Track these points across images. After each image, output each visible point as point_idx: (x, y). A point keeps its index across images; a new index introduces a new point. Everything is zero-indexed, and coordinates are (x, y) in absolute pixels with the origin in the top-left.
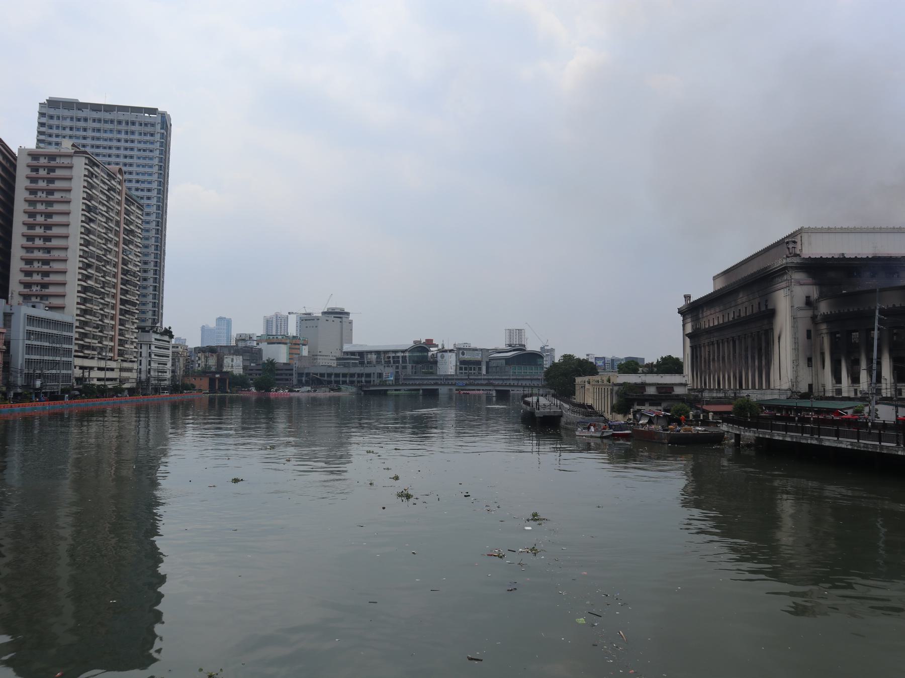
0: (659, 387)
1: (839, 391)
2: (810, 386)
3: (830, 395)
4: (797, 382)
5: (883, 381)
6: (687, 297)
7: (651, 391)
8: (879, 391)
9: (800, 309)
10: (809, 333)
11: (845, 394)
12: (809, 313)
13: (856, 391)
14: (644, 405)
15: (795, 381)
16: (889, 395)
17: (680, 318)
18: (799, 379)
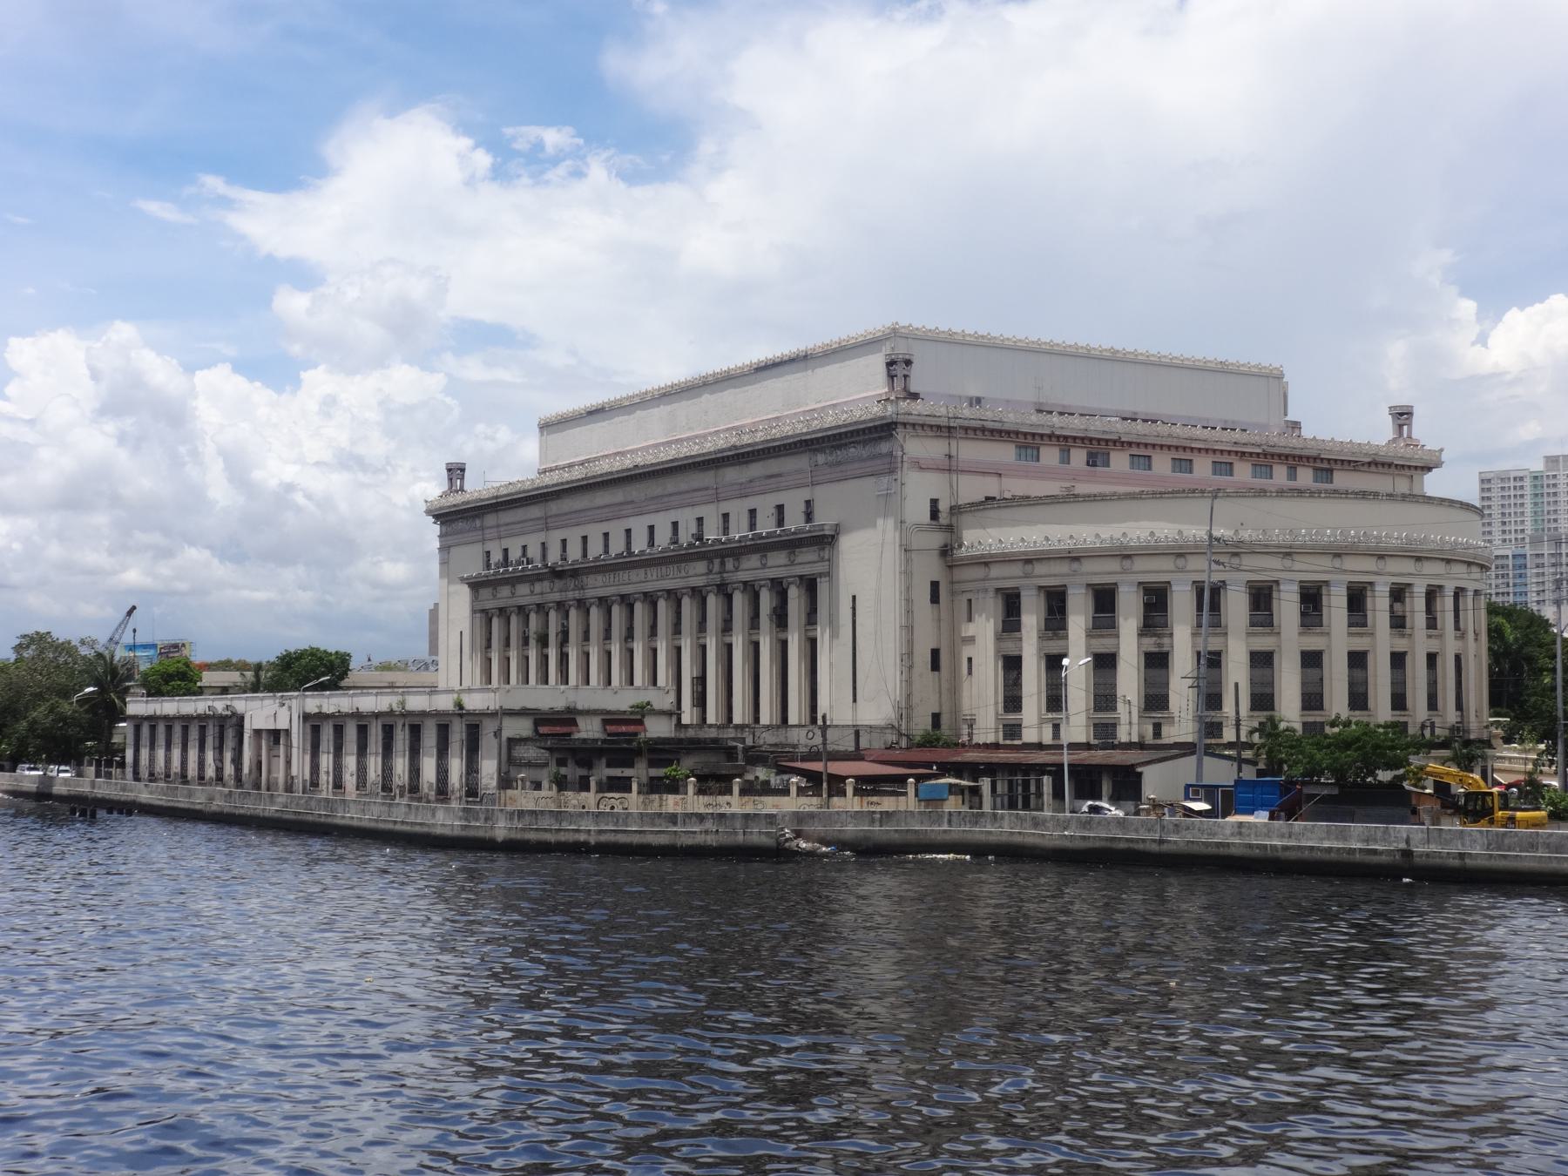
0: (610, 719)
1: (1013, 730)
2: (936, 718)
3: (991, 739)
4: (909, 707)
5: (1120, 706)
6: (456, 472)
7: (589, 729)
8: (1214, 729)
9: (919, 527)
10: (935, 586)
11: (1029, 736)
12: (937, 539)
13: (1056, 727)
14: (631, 765)
15: (906, 708)
16: (1135, 739)
17: (433, 530)
18: (915, 700)
